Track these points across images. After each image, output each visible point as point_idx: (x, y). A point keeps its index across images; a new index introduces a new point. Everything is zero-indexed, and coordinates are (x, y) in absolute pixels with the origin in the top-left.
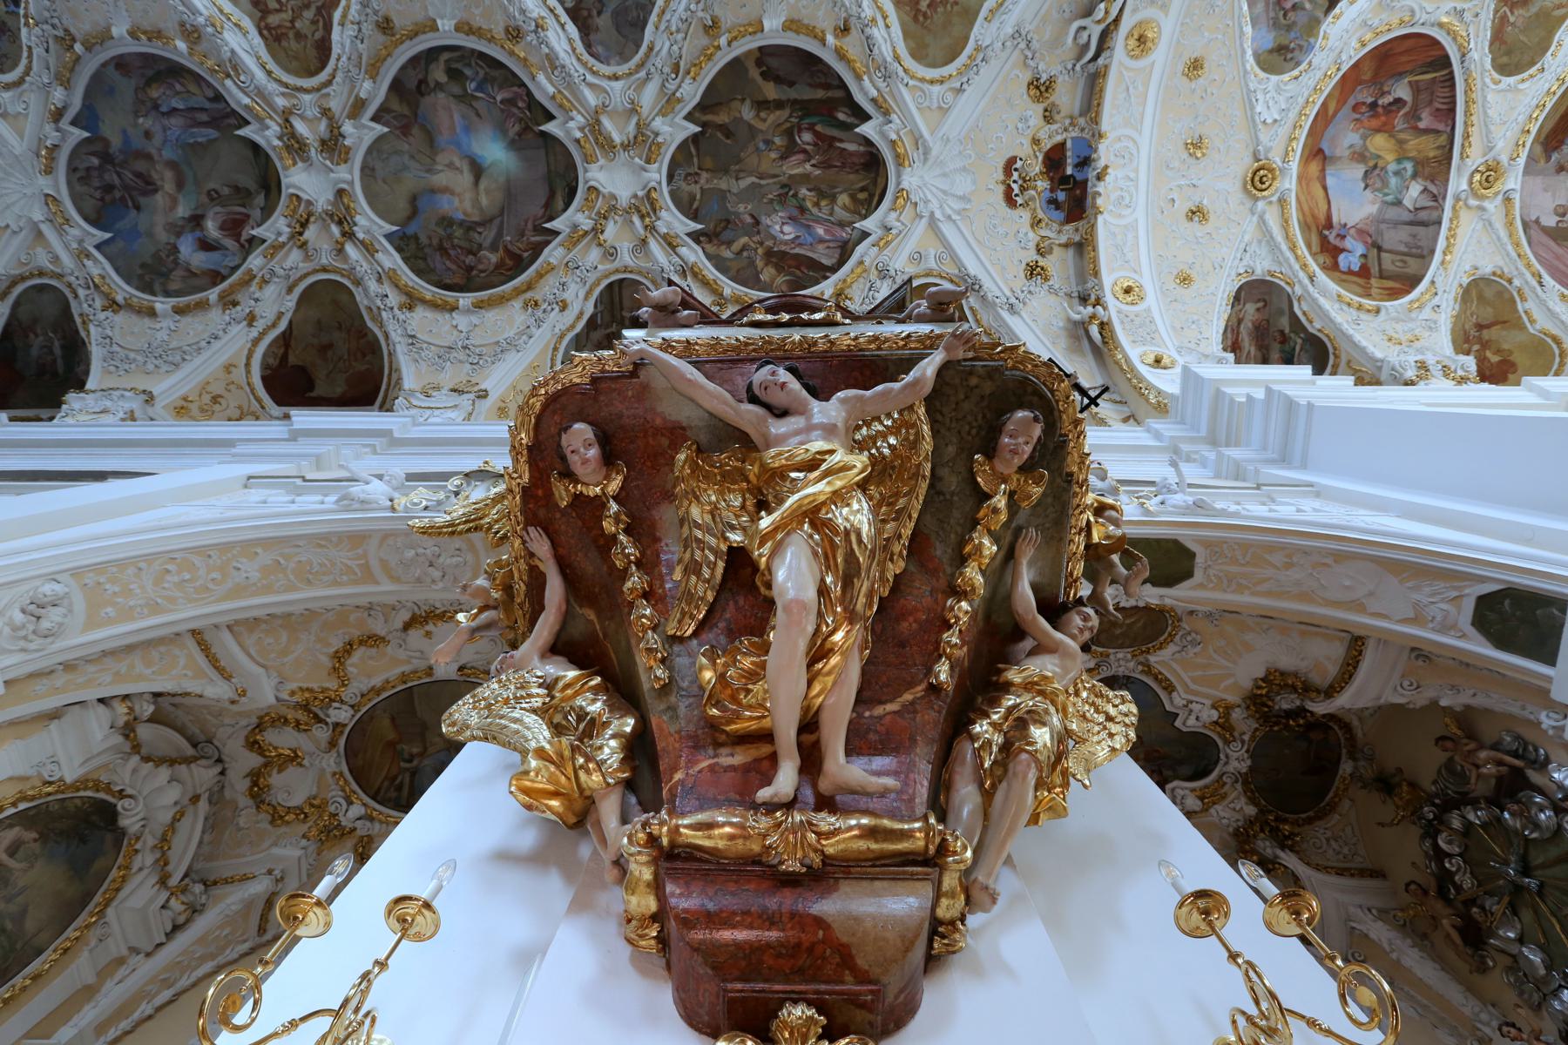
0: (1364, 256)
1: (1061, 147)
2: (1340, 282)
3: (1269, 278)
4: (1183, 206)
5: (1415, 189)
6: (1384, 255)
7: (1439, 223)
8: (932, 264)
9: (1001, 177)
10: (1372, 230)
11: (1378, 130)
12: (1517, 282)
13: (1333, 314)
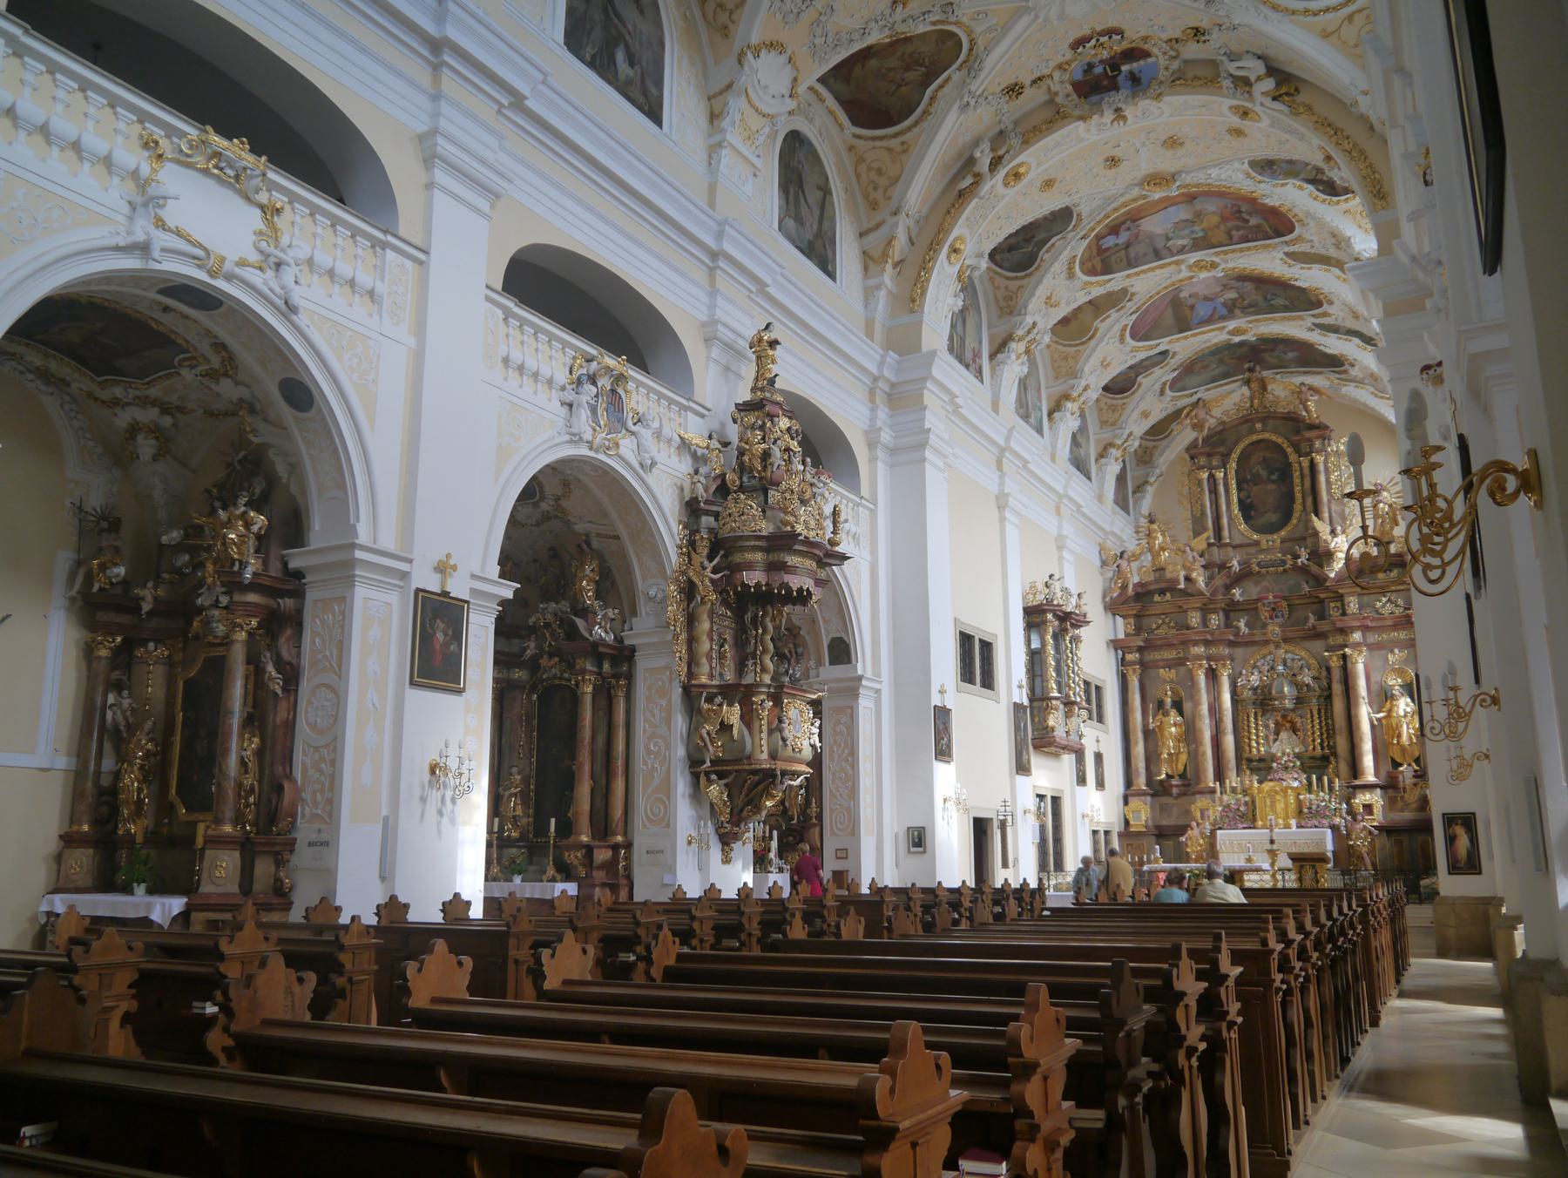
0: (1117, 245)
1: (1147, 54)
2: (1089, 247)
3: (1075, 214)
4: (1117, 153)
5: (1181, 242)
6: (1123, 251)
7: (1161, 259)
8: (979, 29)
9: (1099, 28)
10: (1140, 238)
11: (1222, 216)
12: (1129, 304)
13: (1056, 264)
